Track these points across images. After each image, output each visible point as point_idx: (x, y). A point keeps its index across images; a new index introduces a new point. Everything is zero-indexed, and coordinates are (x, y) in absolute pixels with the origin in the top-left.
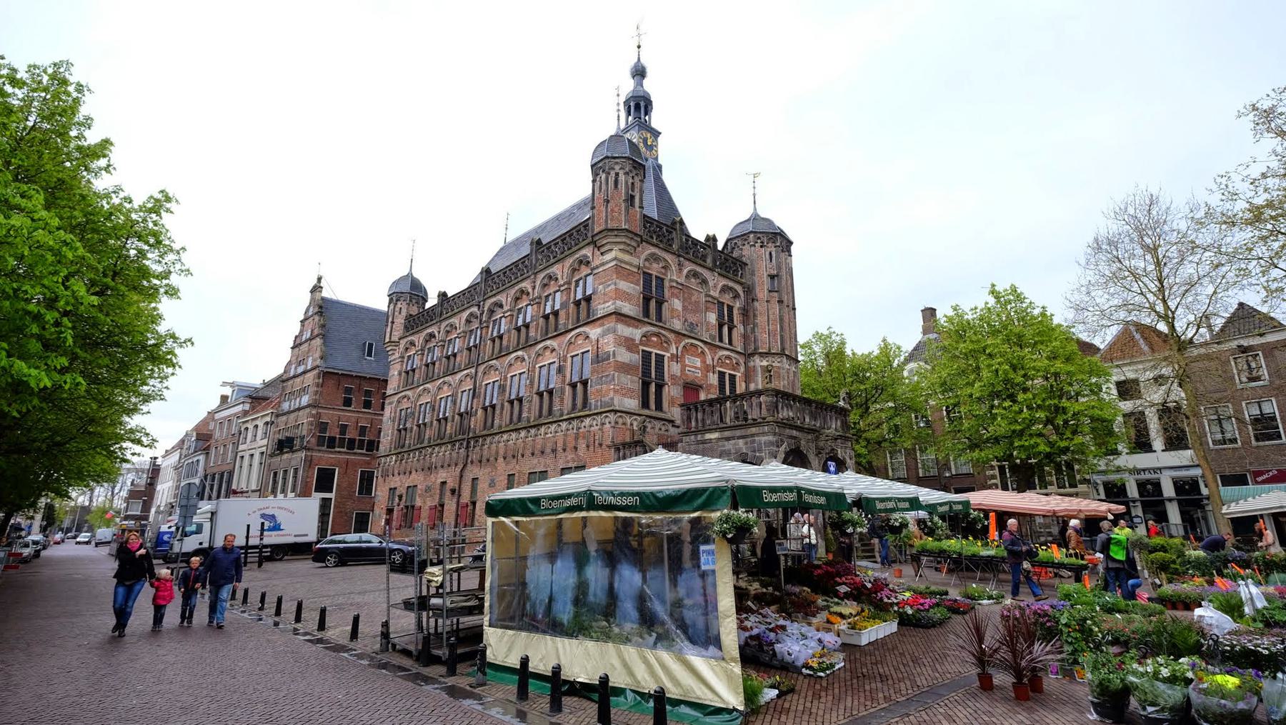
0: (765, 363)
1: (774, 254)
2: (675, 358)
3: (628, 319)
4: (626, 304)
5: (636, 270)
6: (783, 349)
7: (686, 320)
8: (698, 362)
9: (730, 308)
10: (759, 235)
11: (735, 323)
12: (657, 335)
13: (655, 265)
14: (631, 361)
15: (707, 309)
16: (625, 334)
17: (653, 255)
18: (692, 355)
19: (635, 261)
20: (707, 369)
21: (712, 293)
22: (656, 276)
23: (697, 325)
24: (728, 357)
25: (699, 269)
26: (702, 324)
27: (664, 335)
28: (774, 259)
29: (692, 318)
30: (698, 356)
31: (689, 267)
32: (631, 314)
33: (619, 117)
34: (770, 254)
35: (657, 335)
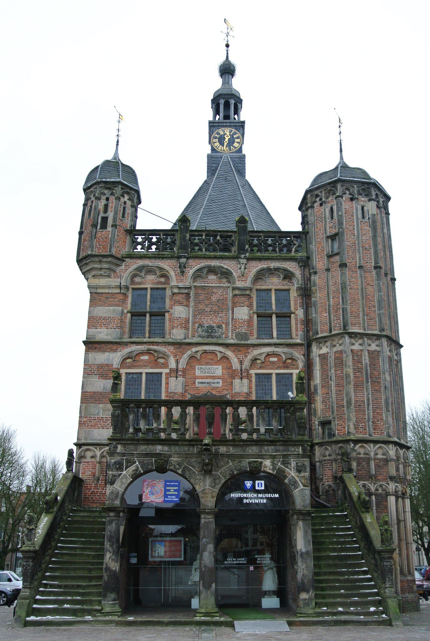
0: (324, 350)
1: (335, 208)
2: (175, 372)
3: (103, 345)
4: (104, 330)
5: (118, 291)
6: (345, 327)
7: (201, 326)
8: (218, 370)
9: (283, 293)
10: (316, 192)
11: (292, 309)
12: (148, 352)
13: (151, 277)
14: (104, 388)
15: (234, 305)
16: (98, 362)
17: (140, 269)
18: (207, 364)
19: (114, 281)
20: (232, 374)
21: (239, 284)
22: (152, 289)
23: (219, 327)
24: (268, 355)
25: (214, 263)
26: (227, 324)
27: (155, 351)
28: (335, 214)
29: (208, 321)
30: (217, 363)
31: (195, 266)
32: (109, 338)
33: (118, 142)
34: (332, 209)
35: (148, 352)
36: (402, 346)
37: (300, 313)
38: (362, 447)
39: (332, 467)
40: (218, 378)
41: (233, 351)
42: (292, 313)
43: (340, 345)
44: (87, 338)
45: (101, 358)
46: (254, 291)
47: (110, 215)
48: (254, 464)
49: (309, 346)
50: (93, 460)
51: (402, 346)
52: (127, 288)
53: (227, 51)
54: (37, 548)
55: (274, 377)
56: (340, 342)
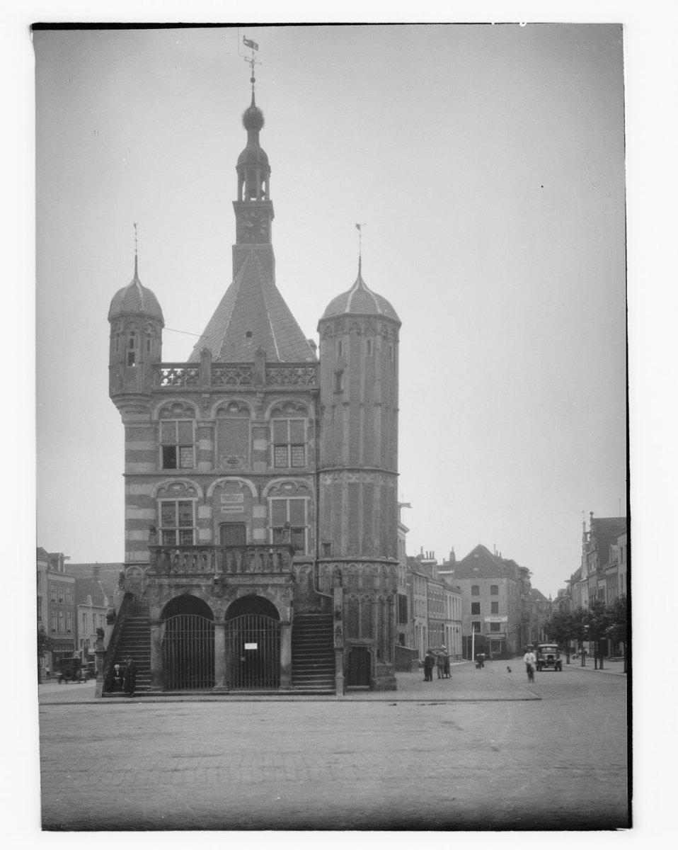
2: (204, 501)
15: (254, 438)
20: (250, 502)
36: (399, 475)
37: (312, 443)
38: (353, 565)
40: (240, 504)
41: (254, 481)
44: (126, 470)
45: (139, 490)
46: (272, 424)
47: (137, 351)
49: (318, 474)
50: (139, 576)
51: (399, 475)
52: (157, 423)
53: (253, 88)
54: (106, 650)
55: (288, 502)
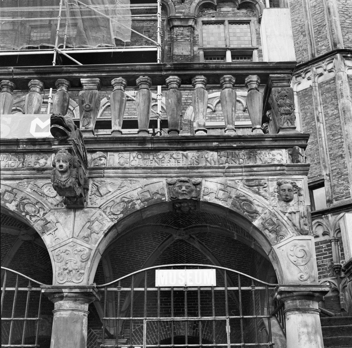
0: (305, 84)
39: (331, 253)
42: (254, 49)
43: (330, 71)
48: (180, 187)
56: (330, 66)
